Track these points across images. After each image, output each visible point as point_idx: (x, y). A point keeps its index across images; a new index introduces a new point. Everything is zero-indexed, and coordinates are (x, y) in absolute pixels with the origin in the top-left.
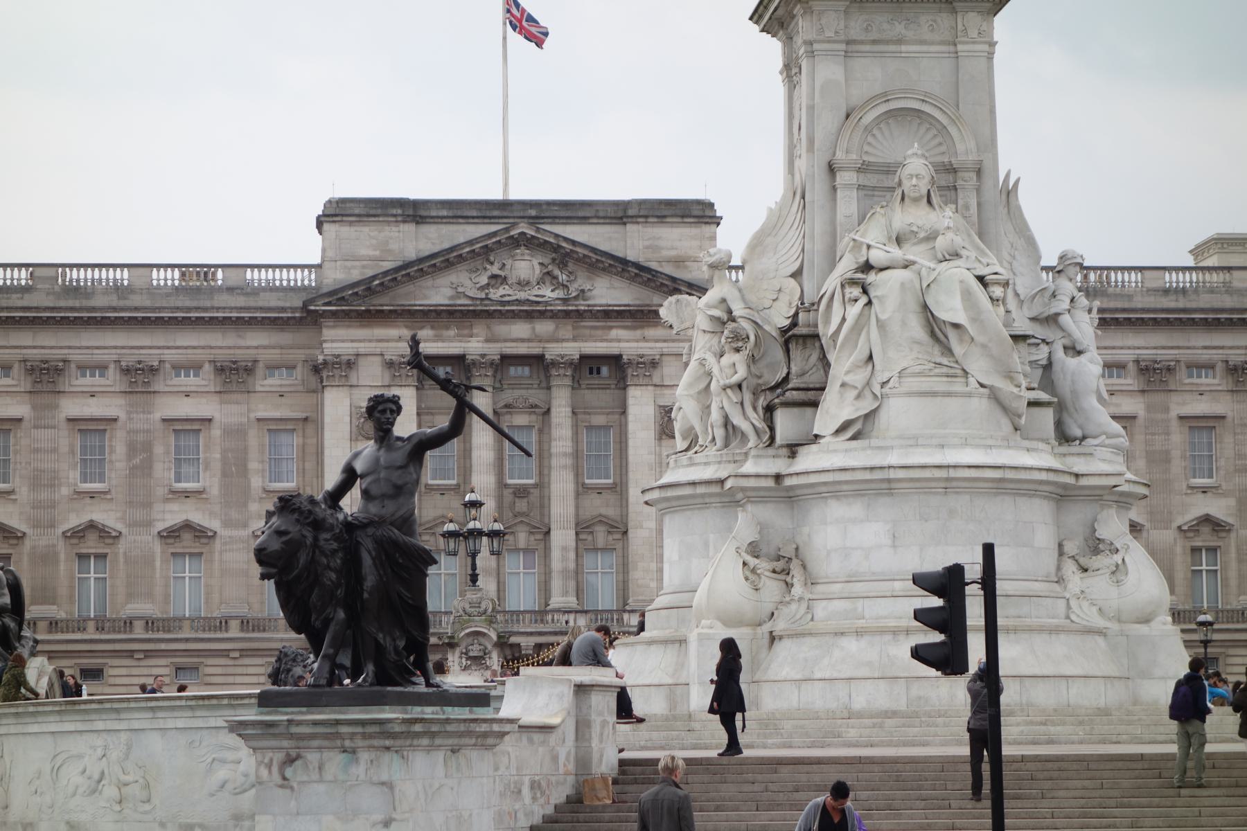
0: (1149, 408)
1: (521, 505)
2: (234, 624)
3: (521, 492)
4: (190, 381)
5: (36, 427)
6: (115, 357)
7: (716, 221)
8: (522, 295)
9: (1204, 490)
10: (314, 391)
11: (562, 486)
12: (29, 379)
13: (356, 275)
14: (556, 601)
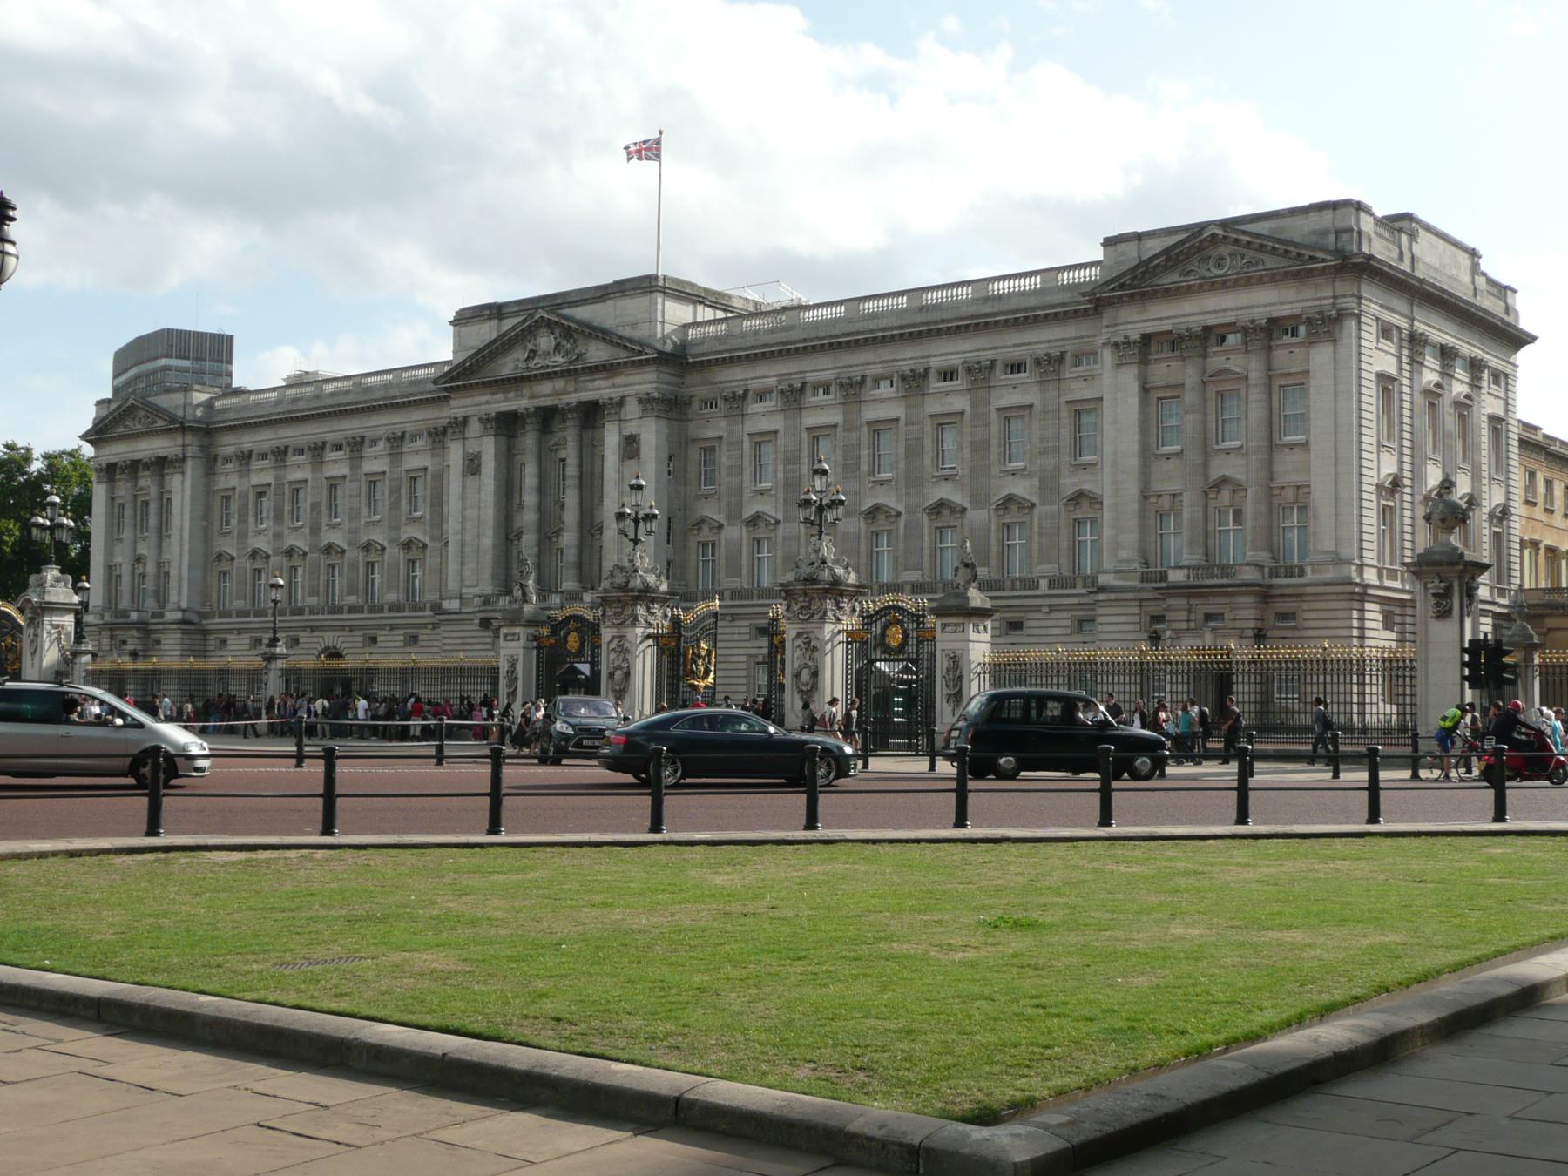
8: (546, 362)
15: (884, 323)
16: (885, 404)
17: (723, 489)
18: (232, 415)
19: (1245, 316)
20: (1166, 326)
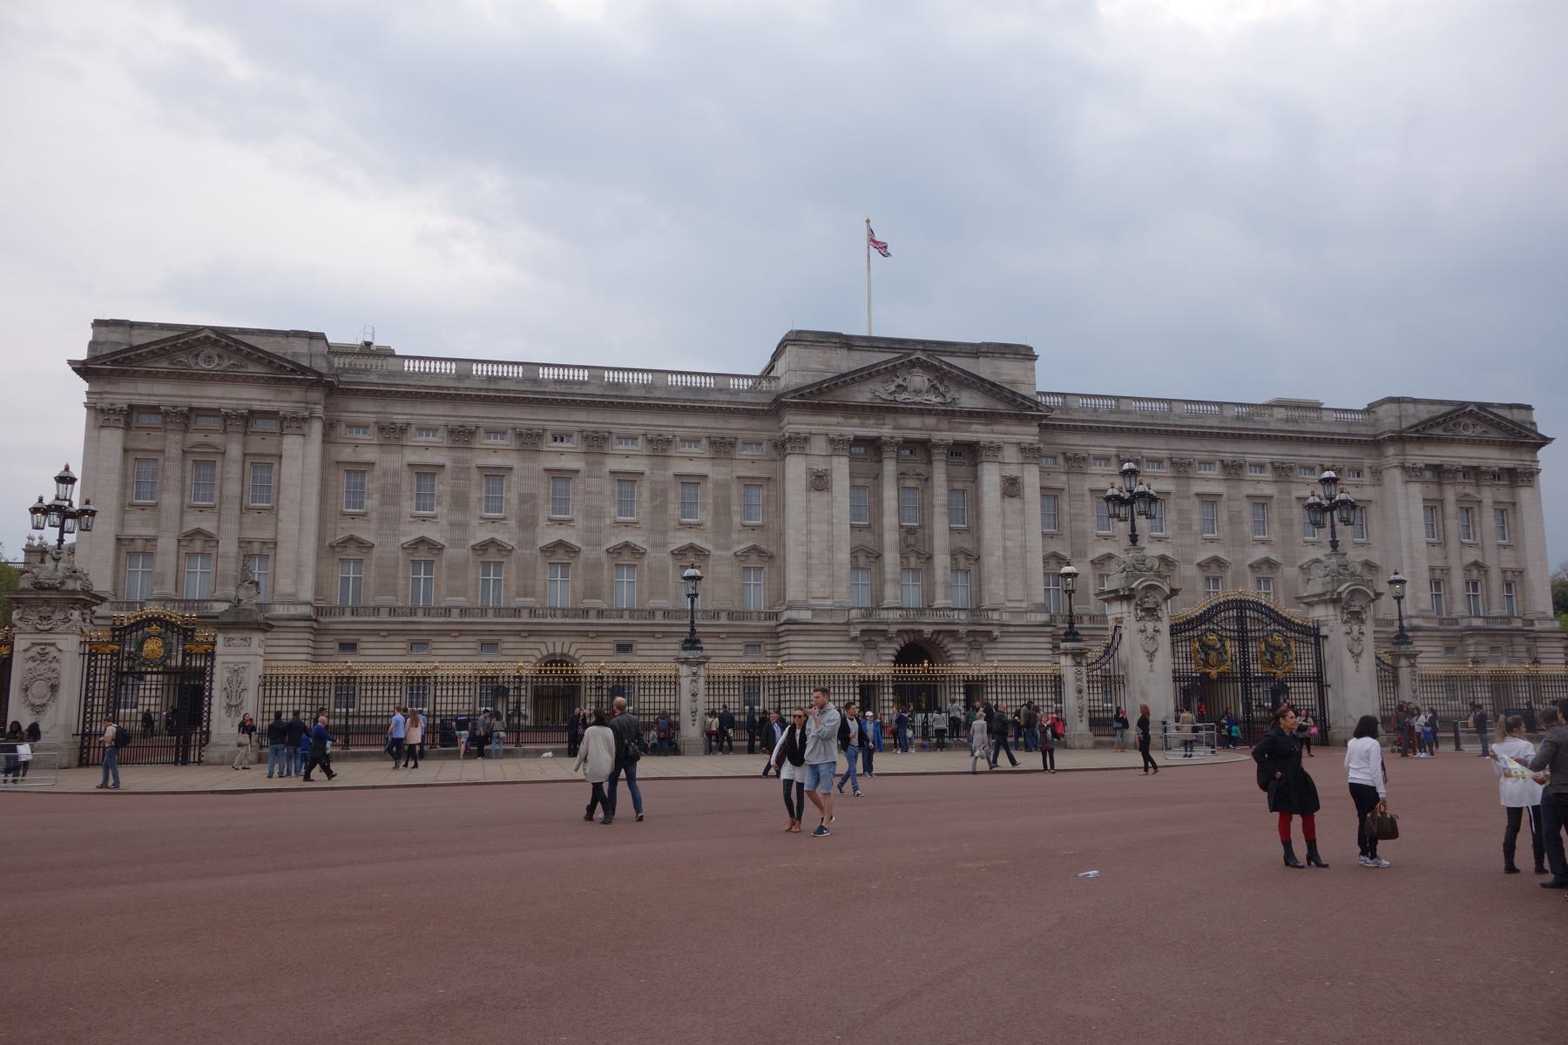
0: (1280, 492)
1: (911, 540)
2: (724, 615)
3: (911, 531)
4: (693, 450)
7: (1033, 358)
8: (917, 399)
9: (1313, 544)
11: (940, 525)
13: (810, 381)
14: (940, 602)
15: (1209, 423)
16: (1210, 482)
17: (1066, 532)
18: (374, 379)
19: (1483, 464)
20: (1437, 461)
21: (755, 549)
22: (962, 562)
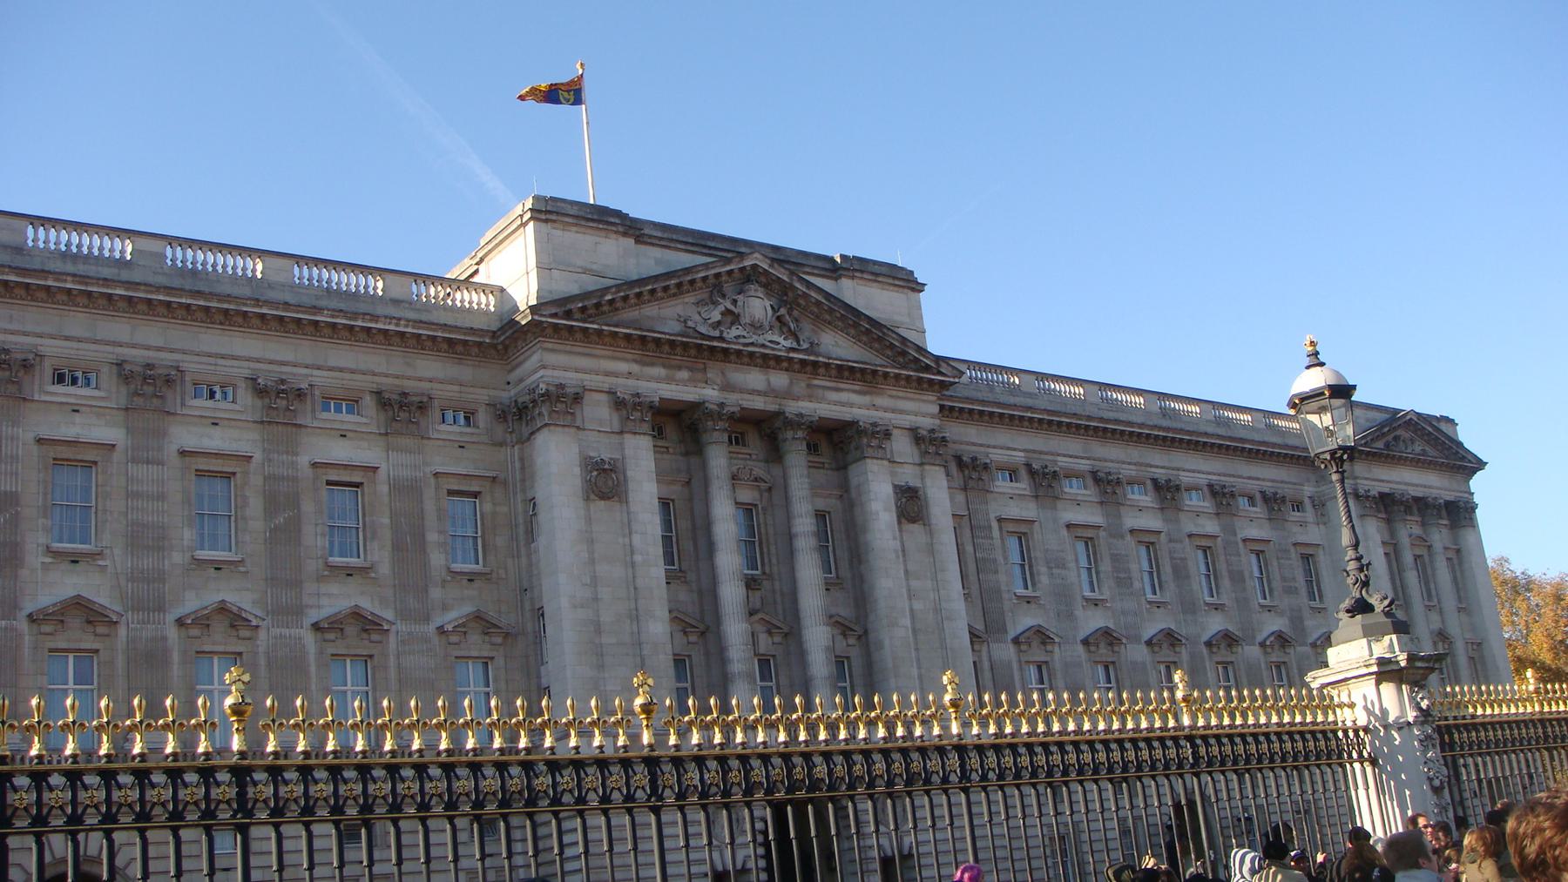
1: (756, 597)
4: (347, 419)
5: (135, 461)
6: (247, 373)
10: (501, 444)
12: (123, 390)
13: (574, 289)
20: (1387, 490)
21: (478, 617)
22: (841, 644)
